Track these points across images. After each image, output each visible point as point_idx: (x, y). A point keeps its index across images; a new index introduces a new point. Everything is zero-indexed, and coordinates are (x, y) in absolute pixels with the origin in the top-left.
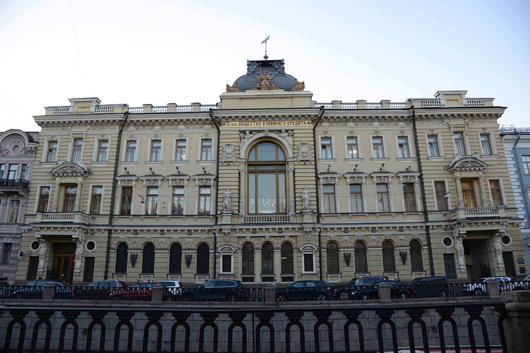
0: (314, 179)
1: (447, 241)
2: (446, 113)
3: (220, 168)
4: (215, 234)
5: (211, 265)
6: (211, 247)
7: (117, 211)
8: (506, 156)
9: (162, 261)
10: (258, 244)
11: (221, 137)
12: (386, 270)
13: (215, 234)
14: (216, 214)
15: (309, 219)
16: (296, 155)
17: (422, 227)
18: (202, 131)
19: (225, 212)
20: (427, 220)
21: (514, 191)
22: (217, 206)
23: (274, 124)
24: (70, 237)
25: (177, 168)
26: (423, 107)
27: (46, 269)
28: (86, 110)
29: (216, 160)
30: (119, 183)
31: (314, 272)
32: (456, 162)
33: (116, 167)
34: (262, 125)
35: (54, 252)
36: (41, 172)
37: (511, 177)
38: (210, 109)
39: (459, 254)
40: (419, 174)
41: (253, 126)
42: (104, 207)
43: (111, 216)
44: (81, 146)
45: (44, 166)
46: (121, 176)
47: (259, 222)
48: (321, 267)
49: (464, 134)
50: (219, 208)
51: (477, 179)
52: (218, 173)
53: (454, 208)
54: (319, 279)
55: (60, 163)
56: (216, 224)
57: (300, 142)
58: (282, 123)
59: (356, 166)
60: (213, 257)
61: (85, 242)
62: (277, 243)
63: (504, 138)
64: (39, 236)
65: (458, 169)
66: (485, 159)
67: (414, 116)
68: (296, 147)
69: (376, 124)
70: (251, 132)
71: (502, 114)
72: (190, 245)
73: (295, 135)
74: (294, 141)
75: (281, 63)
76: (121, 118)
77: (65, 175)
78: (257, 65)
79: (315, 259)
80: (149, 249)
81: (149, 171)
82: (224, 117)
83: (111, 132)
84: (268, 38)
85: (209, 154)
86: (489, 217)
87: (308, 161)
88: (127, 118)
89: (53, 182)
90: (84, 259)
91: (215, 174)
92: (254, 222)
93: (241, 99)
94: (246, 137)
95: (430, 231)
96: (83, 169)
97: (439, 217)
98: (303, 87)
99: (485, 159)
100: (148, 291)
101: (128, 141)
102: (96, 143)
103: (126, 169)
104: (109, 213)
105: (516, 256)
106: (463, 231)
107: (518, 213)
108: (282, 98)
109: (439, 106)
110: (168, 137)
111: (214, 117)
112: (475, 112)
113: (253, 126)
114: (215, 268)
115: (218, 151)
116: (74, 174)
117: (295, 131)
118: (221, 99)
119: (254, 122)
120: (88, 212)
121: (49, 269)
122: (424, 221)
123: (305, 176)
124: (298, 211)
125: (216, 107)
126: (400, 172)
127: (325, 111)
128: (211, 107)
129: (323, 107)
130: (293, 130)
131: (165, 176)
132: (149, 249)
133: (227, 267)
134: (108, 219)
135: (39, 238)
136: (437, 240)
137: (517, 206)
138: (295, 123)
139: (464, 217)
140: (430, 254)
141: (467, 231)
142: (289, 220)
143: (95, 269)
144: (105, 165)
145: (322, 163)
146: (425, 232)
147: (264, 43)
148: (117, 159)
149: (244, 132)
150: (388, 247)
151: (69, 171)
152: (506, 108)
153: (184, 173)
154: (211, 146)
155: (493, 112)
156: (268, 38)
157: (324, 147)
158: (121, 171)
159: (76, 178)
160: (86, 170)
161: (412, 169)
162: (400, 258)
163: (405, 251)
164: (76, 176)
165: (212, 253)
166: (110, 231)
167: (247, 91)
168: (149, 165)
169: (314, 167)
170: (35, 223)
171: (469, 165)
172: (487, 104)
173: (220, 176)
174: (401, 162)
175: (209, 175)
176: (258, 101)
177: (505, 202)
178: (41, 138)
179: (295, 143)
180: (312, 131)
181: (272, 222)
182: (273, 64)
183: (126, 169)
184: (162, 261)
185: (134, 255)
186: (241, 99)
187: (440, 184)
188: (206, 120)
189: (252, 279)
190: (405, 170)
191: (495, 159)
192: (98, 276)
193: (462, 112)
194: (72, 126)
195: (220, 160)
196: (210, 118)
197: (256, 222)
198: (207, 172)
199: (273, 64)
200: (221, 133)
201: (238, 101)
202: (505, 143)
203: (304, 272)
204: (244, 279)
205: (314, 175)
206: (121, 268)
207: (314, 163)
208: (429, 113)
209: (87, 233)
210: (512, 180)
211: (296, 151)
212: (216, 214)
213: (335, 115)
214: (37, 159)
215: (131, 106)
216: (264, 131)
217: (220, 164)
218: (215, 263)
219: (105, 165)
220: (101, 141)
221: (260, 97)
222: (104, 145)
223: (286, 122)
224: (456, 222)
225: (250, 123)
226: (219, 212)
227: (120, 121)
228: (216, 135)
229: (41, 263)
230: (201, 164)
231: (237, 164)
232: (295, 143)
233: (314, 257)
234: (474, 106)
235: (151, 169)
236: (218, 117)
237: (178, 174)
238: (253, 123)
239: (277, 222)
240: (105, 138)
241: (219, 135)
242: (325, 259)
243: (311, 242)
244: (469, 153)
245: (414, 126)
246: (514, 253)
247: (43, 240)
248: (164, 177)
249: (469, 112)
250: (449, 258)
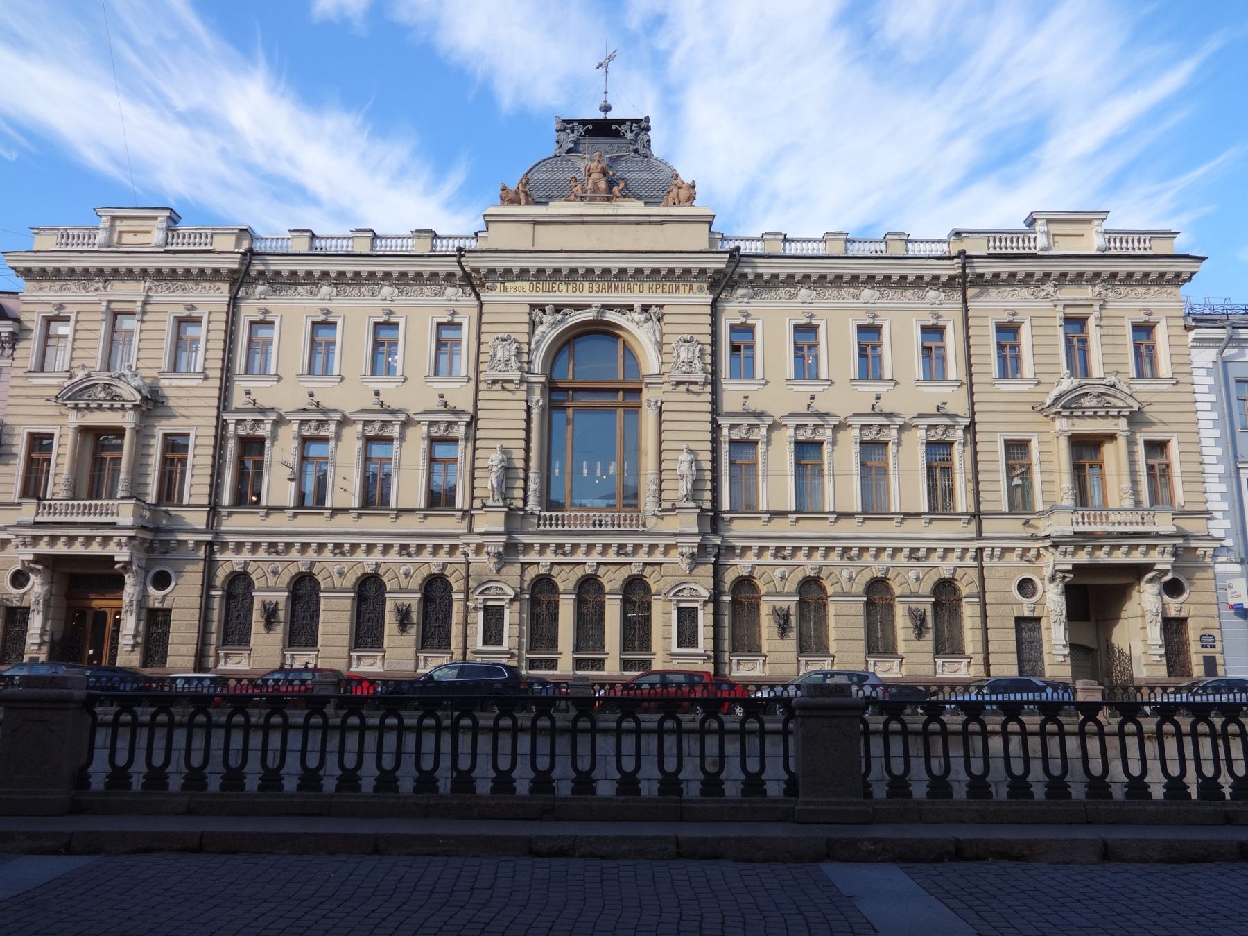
0: (709, 427)
1: (1026, 587)
2: (1048, 269)
3: (481, 395)
4: (466, 554)
5: (456, 629)
6: (457, 585)
7: (226, 499)
8: (1197, 380)
9: (335, 616)
10: (566, 580)
11: (485, 318)
12: (871, 649)
13: (466, 554)
14: (472, 508)
15: (688, 522)
16: (665, 368)
17: (965, 550)
18: (441, 302)
19: (490, 503)
20: (980, 536)
21: (1208, 469)
22: (473, 488)
23: (616, 289)
24: (110, 560)
25: (377, 394)
26: (992, 251)
27: (46, 638)
28: (141, 239)
29: (472, 375)
30: (231, 427)
31: (700, 650)
32: (1061, 396)
34: (586, 293)
35: (68, 596)
36: (28, 397)
37: (1203, 433)
38: (460, 249)
39: (1053, 619)
40: (967, 422)
41: (564, 294)
42: (195, 486)
43: (214, 508)
44: (132, 331)
45: (35, 382)
46: (238, 410)
47: (572, 528)
48: (717, 638)
49: (1091, 324)
50: (476, 493)
51: (1112, 437)
52: (476, 409)
53: (1047, 507)
54: (709, 667)
55: (80, 374)
56: (470, 532)
57: (678, 337)
58: (637, 288)
59: (812, 398)
60: (462, 609)
61: (147, 572)
62: (612, 581)
63: (1192, 334)
64: (31, 557)
65: (1066, 413)
66: (1138, 387)
67: (964, 275)
68: (666, 349)
69: (867, 292)
70: (558, 308)
71: (1192, 274)
72: (403, 582)
73: (666, 319)
74: (662, 335)
75: (641, 126)
76: (232, 263)
77: (94, 405)
78: (582, 129)
79: (704, 620)
80: (304, 590)
81: (308, 399)
82: (492, 271)
83: (211, 300)
85: (455, 358)
86: (1135, 533)
87: (696, 383)
88: (250, 264)
89: (60, 421)
90: (144, 612)
91: (470, 409)
92: (560, 528)
94: (545, 319)
95: (986, 561)
96: (140, 392)
97: (1013, 526)
98: (691, 199)
99: (1138, 387)
100: (303, 688)
101: (252, 323)
102: (169, 326)
103: (248, 393)
104: (205, 501)
105: (1193, 632)
106: (1067, 563)
107: (1211, 524)
108: (638, 223)
109: (1033, 251)
110: (356, 314)
111: (468, 269)
112: (1122, 268)
113: (564, 294)
114: (465, 636)
115: (478, 353)
116: (117, 405)
117: (665, 310)
118: (487, 223)
119: (567, 283)
120: (152, 499)
121: (58, 636)
122: (974, 535)
123: (690, 419)
124: (666, 505)
125: (474, 242)
126: (921, 416)
127: (744, 259)
128: (462, 243)
129: (738, 249)
130: (661, 306)
131: (346, 413)
132: (304, 590)
133: (493, 634)
134: (205, 515)
135: (30, 561)
137: (1210, 506)
138: (667, 289)
139: (1069, 530)
141: (1075, 566)
142: (644, 525)
143: (173, 637)
144: (194, 383)
145: (730, 388)
146: (975, 564)
147: (602, 70)
149: (542, 308)
150: (878, 594)
151: (102, 395)
152: (1204, 259)
153: (394, 406)
154: (458, 343)
155: (1170, 268)
157: (735, 349)
158: (238, 399)
159: (121, 413)
160: (145, 393)
161: (950, 409)
162: (909, 624)
163: (921, 608)
164: (123, 408)
165: (458, 600)
166: (210, 544)
167: (551, 203)
168: (307, 384)
169: (708, 398)
170: (19, 526)
171: (1094, 403)
172: (1159, 247)
173: (480, 414)
174: (925, 389)
175: (454, 412)
176: (580, 229)
177: (1179, 498)
178: (24, 308)
179: (665, 339)
180: (708, 310)
181: (603, 528)
182: (623, 129)
183: (248, 393)
184: (335, 616)
185: (270, 603)
186: (535, 223)
187: (1017, 448)
188: (450, 275)
189: (552, 664)
190: (935, 411)
191: (1165, 387)
192: (180, 655)
193: (1089, 268)
194: (106, 281)
195: (482, 377)
196: (457, 270)
197: (566, 528)
198: (451, 404)
199: (623, 129)
200: (485, 309)
202: (1193, 347)
204: (533, 664)
205: (709, 417)
206: (236, 635)
207: (709, 388)
208: (1004, 268)
209: (150, 549)
210: (1204, 442)
211: (666, 358)
212: (472, 508)
213: (766, 268)
214: (16, 363)
215: (259, 231)
216: (590, 306)
217: (482, 386)
218: (466, 624)
219: (194, 383)
220: (181, 321)
221: (581, 221)
222: (191, 331)
223: (646, 285)
224: (1047, 543)
225: (556, 286)
226: (477, 504)
227: (232, 271)
228: (475, 312)
229: (36, 622)
230: (435, 385)
231: (525, 387)
232: (665, 339)
233: (700, 613)
234: (1124, 252)
235: (311, 395)
236: (477, 270)
237: (378, 407)
238: (563, 287)
239: (616, 528)
240: (195, 314)
241: (481, 314)
242: (726, 621)
243: (696, 580)
244: (1097, 369)
245: (965, 301)
246: (1190, 622)
247: (39, 567)
248: (344, 417)
249: (1106, 268)
250: (1027, 626)
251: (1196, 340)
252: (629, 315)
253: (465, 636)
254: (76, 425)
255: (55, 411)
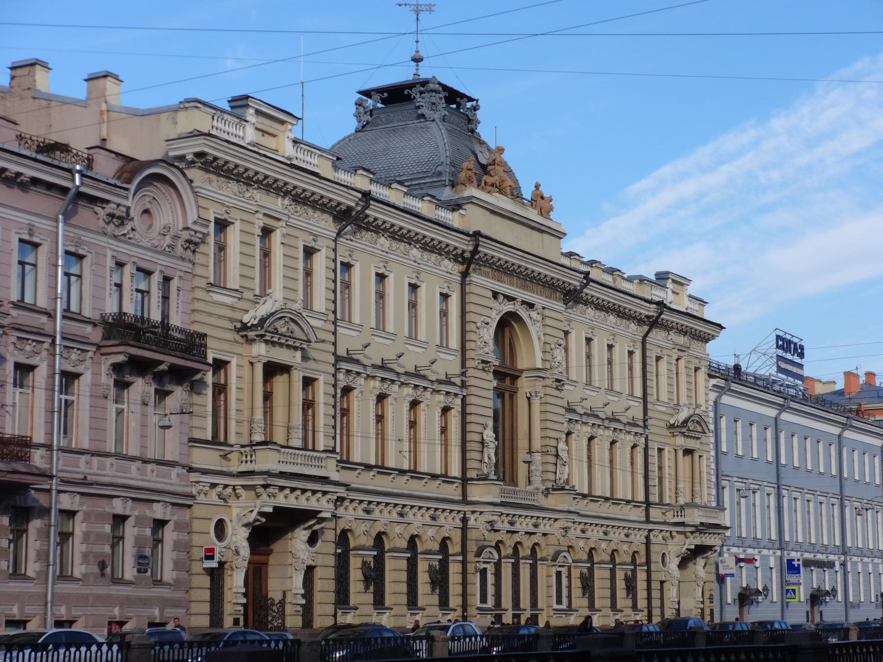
4: (465, 520)
16: (548, 366)
20: (648, 521)
33: (334, 333)
36: (210, 314)
64: (270, 510)
84: (430, 8)
93: (493, 212)
108: (533, 228)
114: (464, 595)
127: (591, 284)
136: (656, 558)
140: (649, 581)
148: (335, 312)
156: (430, 8)
201: (488, 213)
203: (556, 606)
211: (548, 356)
218: (464, 584)
232: (549, 339)
245: (646, 335)
251: (714, 386)
252: (534, 315)
253: (464, 595)
254: (265, 360)
255: (231, 336)
